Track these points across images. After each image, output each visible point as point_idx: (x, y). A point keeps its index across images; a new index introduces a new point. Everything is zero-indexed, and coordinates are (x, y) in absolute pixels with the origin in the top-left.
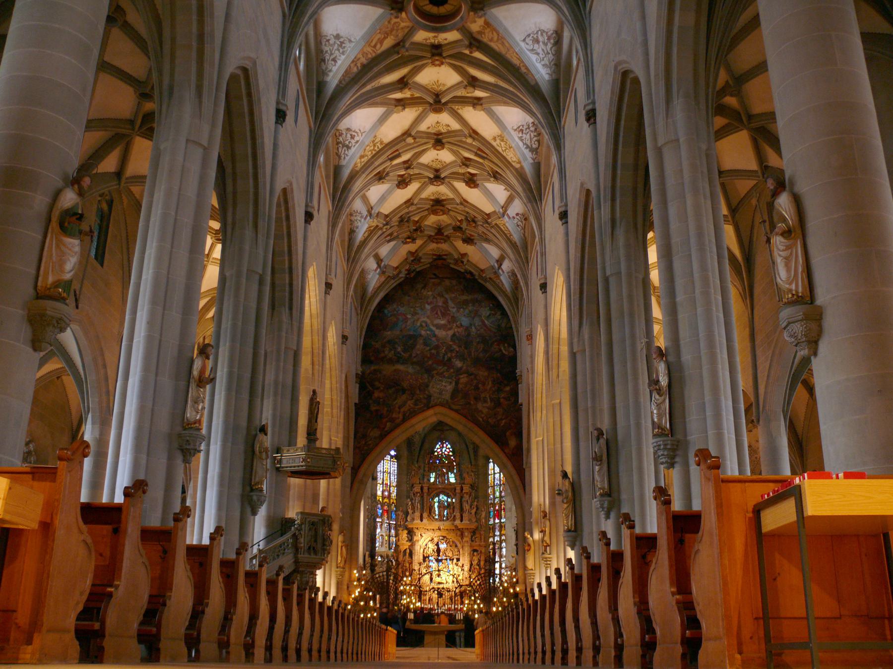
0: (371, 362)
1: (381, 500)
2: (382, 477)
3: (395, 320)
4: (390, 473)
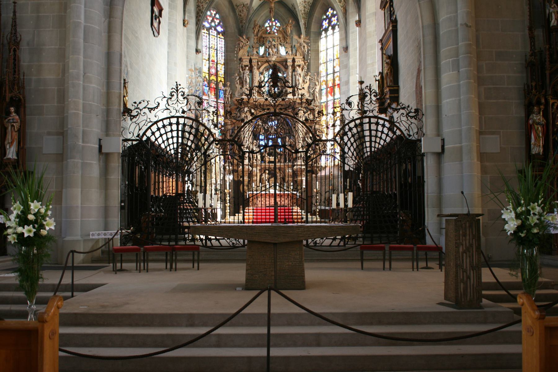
1: (207, 77)
2: (208, 53)
4: (217, 50)
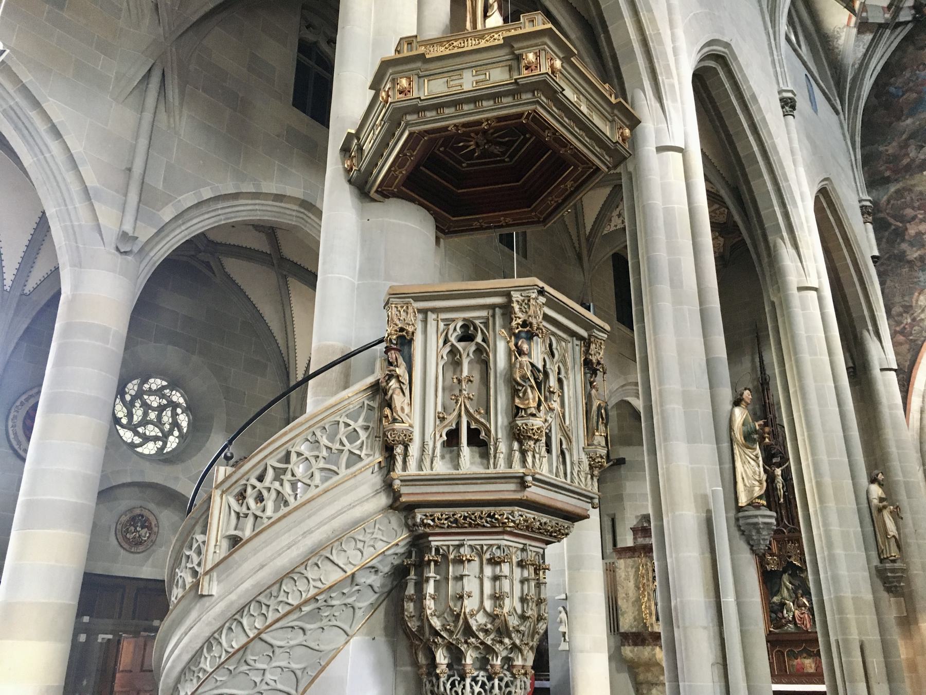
0: (886, 181)
3: (915, 95)
